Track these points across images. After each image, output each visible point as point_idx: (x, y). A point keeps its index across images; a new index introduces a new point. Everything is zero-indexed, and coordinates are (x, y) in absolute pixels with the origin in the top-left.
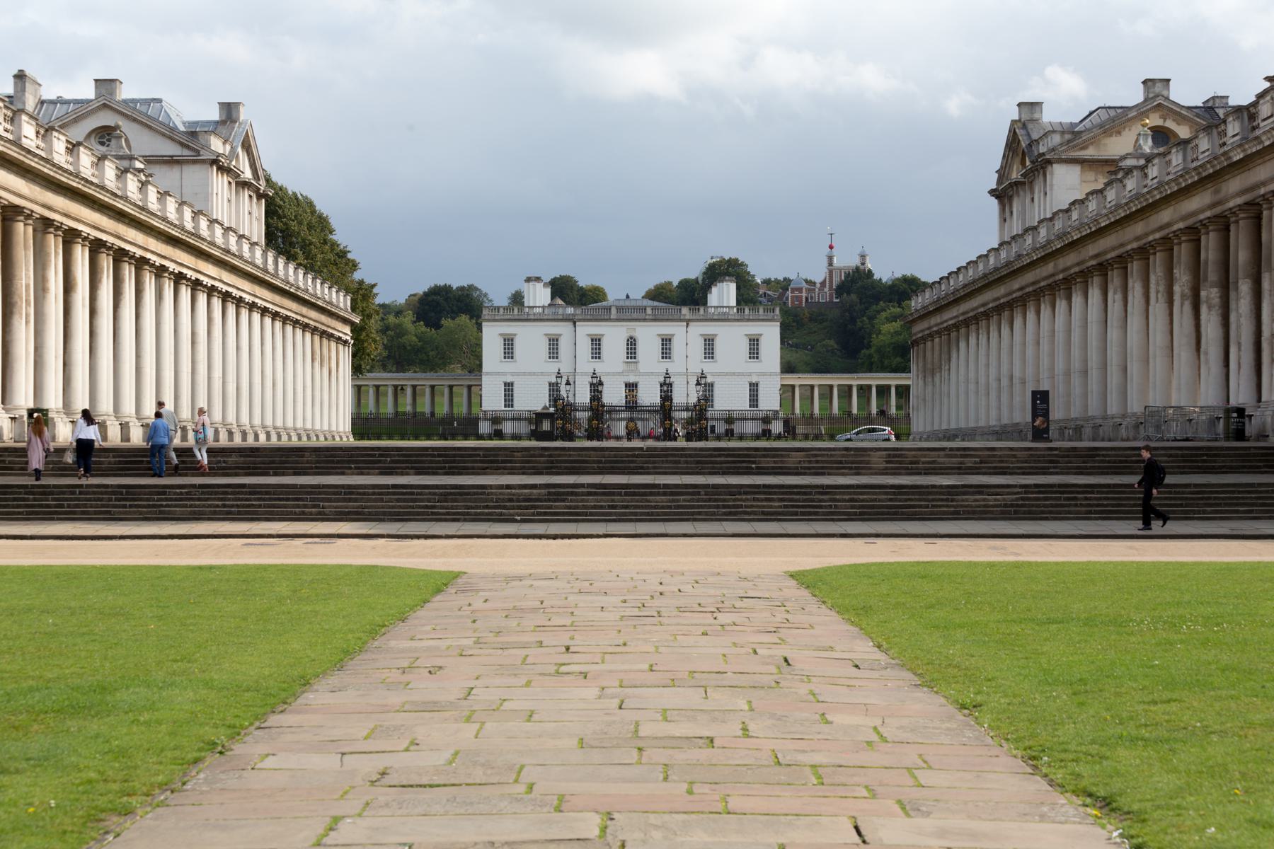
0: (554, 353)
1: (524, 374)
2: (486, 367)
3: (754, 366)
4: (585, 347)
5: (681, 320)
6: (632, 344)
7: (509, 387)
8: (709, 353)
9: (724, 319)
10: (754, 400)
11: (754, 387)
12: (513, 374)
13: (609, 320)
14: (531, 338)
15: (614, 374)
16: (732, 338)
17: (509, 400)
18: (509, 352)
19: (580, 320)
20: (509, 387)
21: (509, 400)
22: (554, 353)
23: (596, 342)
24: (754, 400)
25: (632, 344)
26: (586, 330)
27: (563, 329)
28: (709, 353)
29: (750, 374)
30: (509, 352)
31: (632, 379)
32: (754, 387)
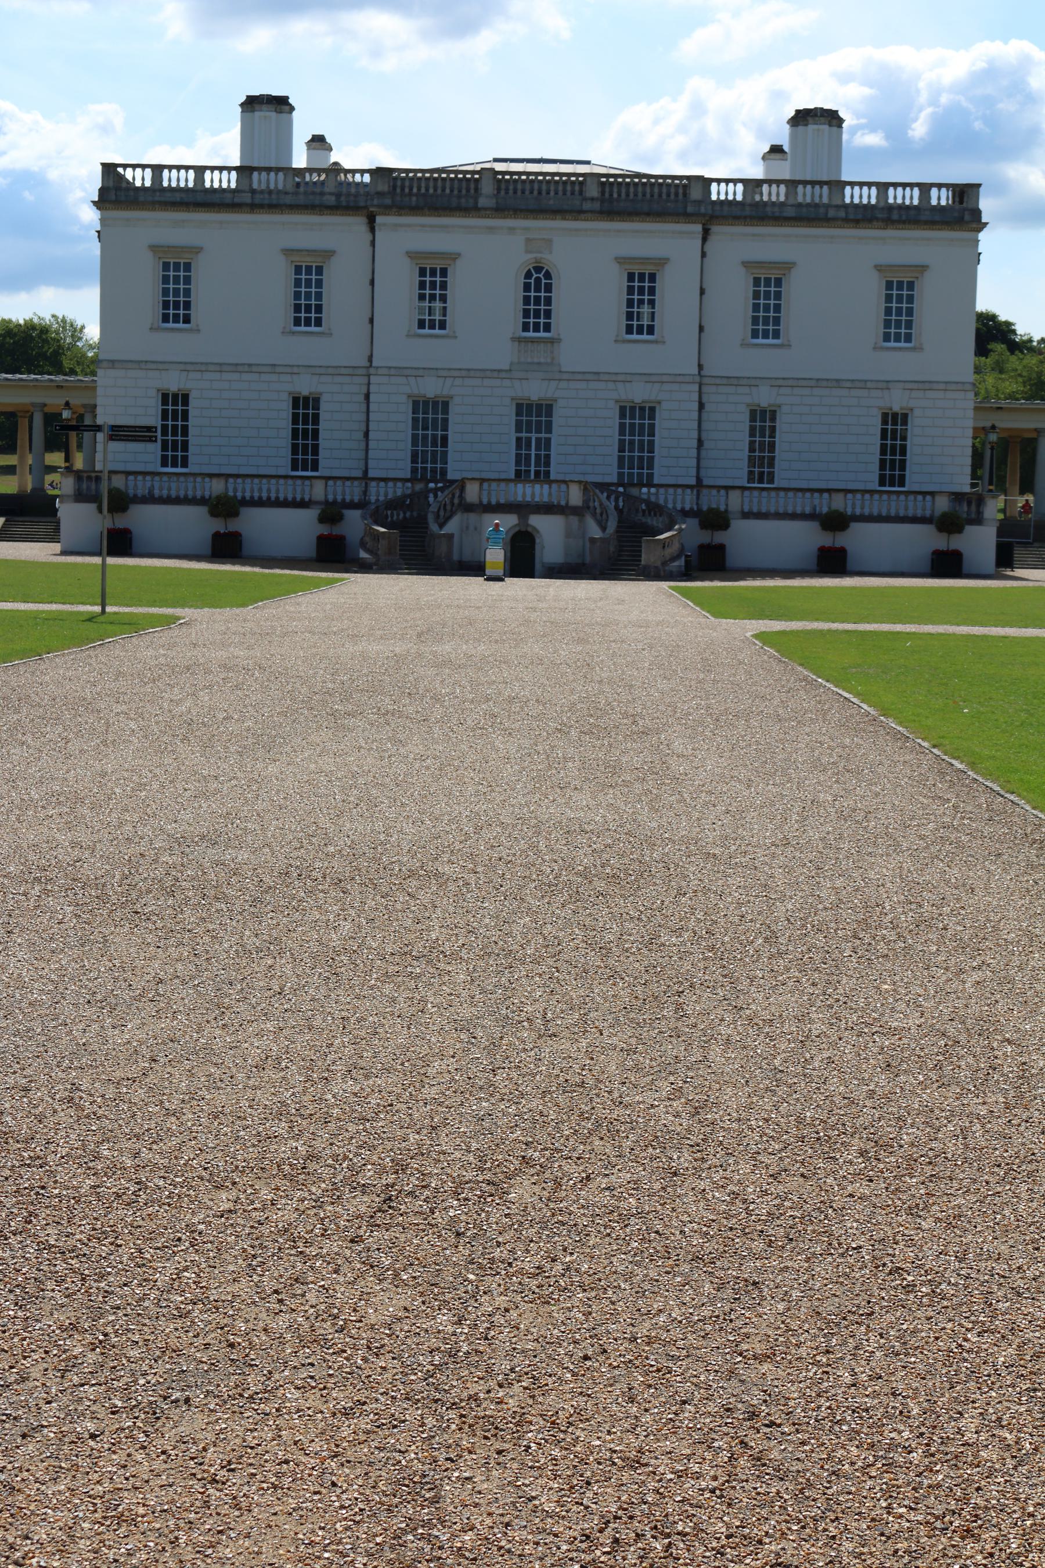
0: (307, 311)
1: (221, 367)
5: (685, 216)
11: (894, 427)
12: (187, 366)
15: (484, 373)
19: (387, 210)
23: (433, 279)
26: (405, 237)
29: (886, 385)
31: (535, 390)
32: (894, 427)
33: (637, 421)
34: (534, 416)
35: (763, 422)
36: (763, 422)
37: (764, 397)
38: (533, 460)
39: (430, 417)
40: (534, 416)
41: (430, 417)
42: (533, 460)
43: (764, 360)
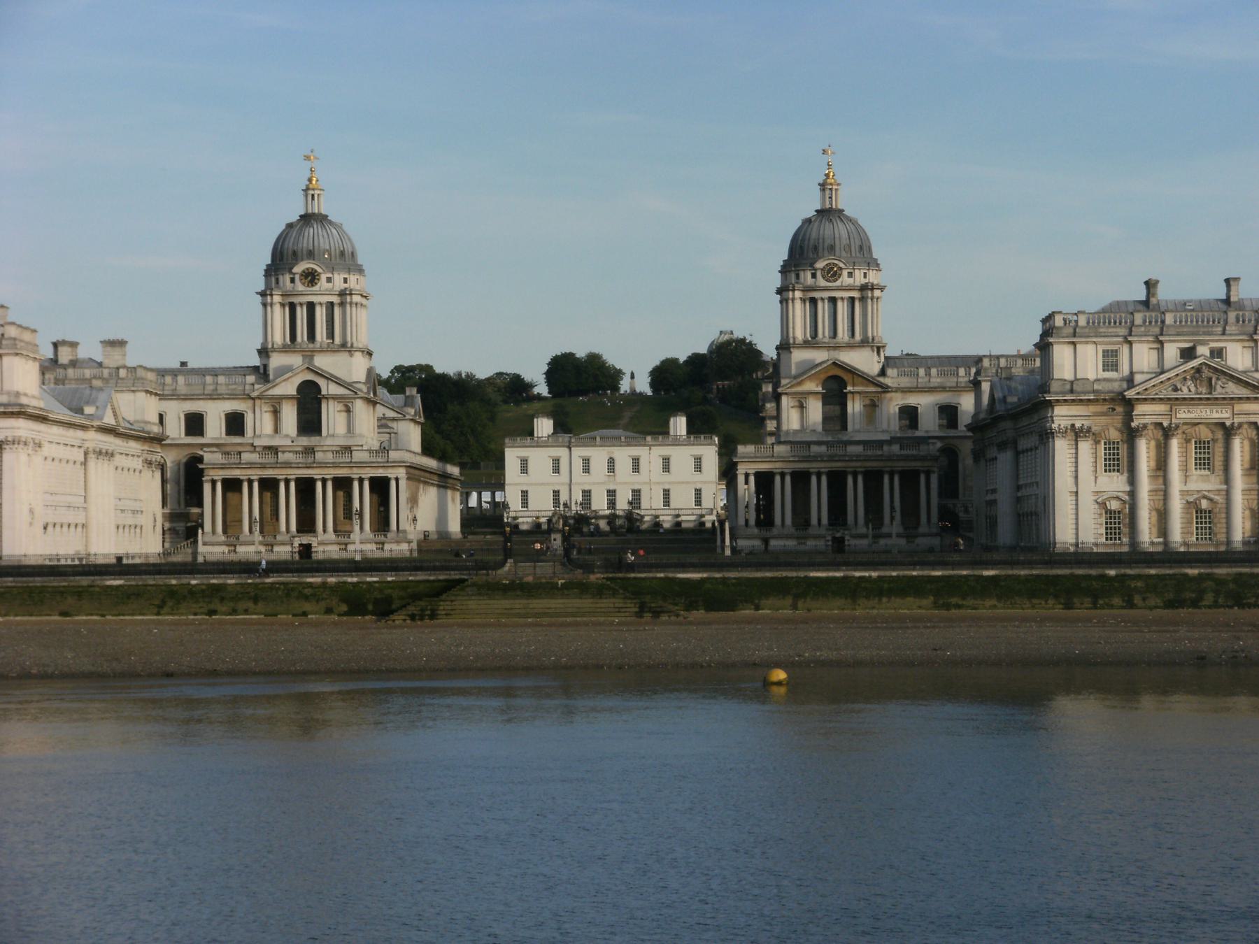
0: (556, 469)
2: (508, 480)
3: (698, 477)
4: (578, 465)
6: (611, 462)
7: (525, 494)
8: (666, 467)
9: (677, 442)
10: (698, 501)
11: (698, 493)
13: (595, 446)
14: (540, 458)
16: (682, 456)
17: (525, 503)
18: (524, 468)
20: (525, 494)
21: (525, 503)
22: (556, 469)
24: (698, 501)
25: (611, 462)
26: (579, 452)
27: (562, 453)
28: (666, 467)
30: (524, 468)
31: (612, 488)
32: (698, 493)
33: (637, 494)
34: (612, 494)
35: (667, 493)
36: (667, 493)
37: (667, 487)
38: (612, 504)
39: (587, 494)
40: (612, 494)
41: (587, 494)
42: (612, 504)
43: (666, 477)
